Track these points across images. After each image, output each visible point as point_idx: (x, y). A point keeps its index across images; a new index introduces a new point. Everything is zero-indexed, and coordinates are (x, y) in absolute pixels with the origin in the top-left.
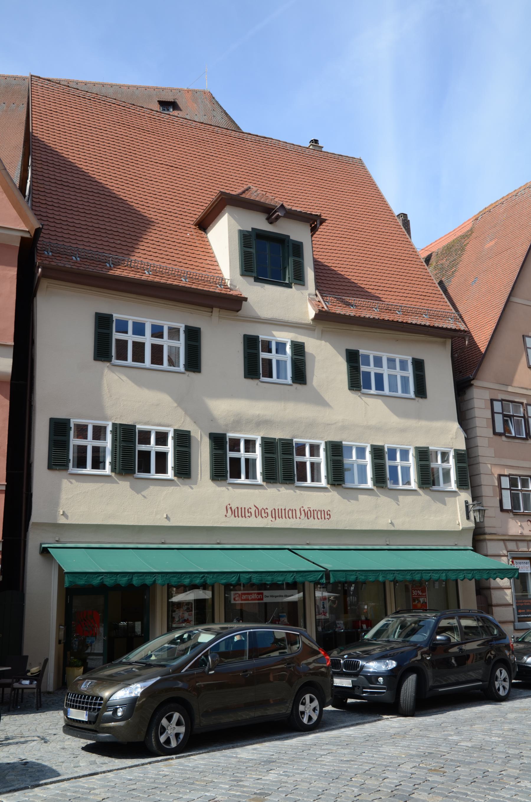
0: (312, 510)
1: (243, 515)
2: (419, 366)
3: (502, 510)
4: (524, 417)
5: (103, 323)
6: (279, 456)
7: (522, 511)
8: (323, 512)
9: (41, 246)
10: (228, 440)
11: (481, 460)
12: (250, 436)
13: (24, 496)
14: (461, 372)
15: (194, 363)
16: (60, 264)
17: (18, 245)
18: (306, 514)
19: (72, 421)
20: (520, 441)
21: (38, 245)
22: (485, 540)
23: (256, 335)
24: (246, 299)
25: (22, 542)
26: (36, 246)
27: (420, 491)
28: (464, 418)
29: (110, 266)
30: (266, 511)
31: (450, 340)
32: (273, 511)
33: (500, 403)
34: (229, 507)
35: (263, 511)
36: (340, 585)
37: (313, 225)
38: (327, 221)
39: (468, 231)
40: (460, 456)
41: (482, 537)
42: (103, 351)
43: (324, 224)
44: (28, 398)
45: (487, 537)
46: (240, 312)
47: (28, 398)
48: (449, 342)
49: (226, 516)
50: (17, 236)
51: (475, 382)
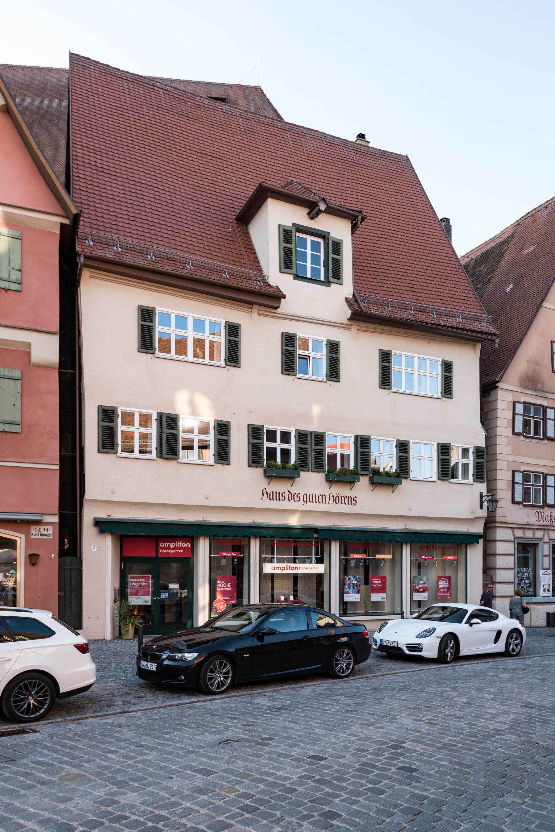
0: (340, 496)
1: (278, 499)
2: (447, 367)
3: (513, 502)
4: (543, 419)
5: (146, 314)
6: (311, 446)
7: (531, 503)
8: (350, 498)
9: (82, 234)
10: (265, 431)
11: (499, 457)
12: (286, 429)
13: (78, 476)
14: (487, 375)
15: (233, 357)
16: (101, 254)
17: (59, 232)
18: (335, 500)
19: (119, 409)
20: (537, 441)
21: (79, 233)
22: (496, 527)
23: (294, 333)
24: (284, 297)
25: (78, 516)
26: (77, 235)
27: (438, 481)
28: (487, 417)
29: (152, 258)
30: (299, 495)
31: (480, 344)
32: (305, 496)
33: (522, 405)
34: (264, 491)
35: (296, 496)
36: (362, 561)
37: (354, 222)
38: (368, 218)
39: (509, 237)
40: (479, 452)
41: (492, 525)
42: (146, 342)
43: (365, 221)
44: (77, 386)
45: (498, 525)
46: (278, 310)
47: (77, 386)
48: (479, 346)
49: (262, 499)
50: (56, 223)
51: (499, 385)
